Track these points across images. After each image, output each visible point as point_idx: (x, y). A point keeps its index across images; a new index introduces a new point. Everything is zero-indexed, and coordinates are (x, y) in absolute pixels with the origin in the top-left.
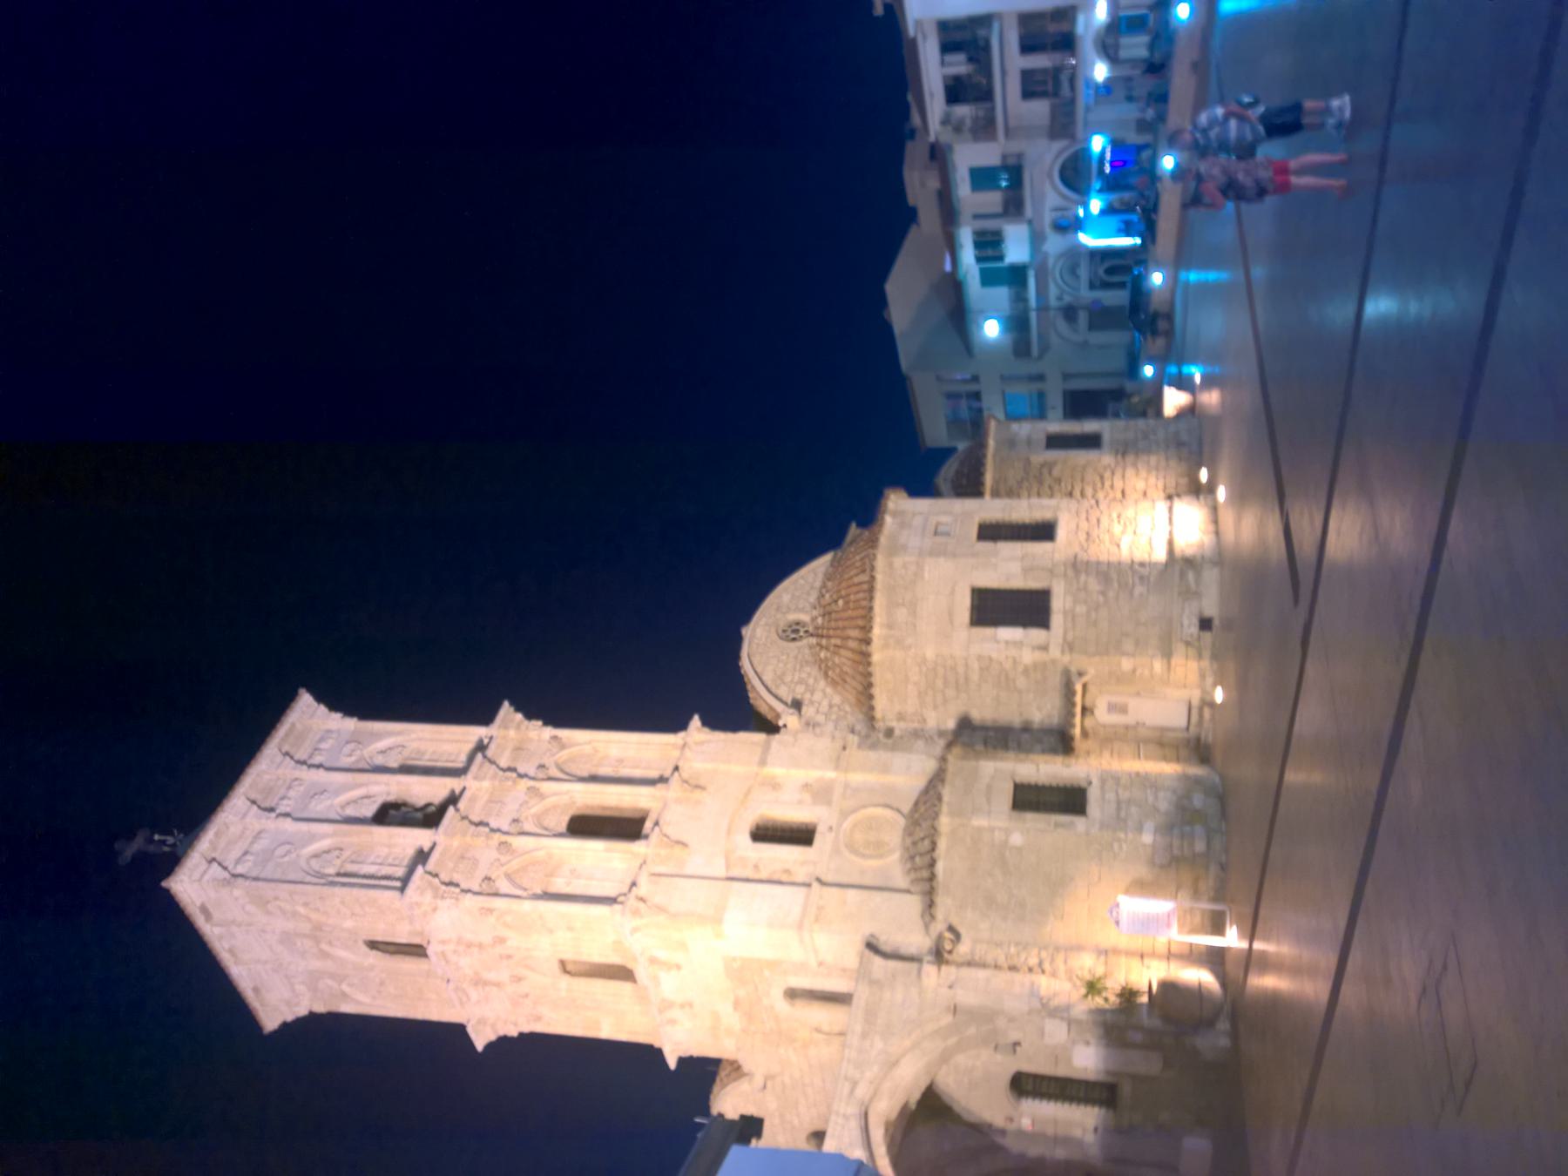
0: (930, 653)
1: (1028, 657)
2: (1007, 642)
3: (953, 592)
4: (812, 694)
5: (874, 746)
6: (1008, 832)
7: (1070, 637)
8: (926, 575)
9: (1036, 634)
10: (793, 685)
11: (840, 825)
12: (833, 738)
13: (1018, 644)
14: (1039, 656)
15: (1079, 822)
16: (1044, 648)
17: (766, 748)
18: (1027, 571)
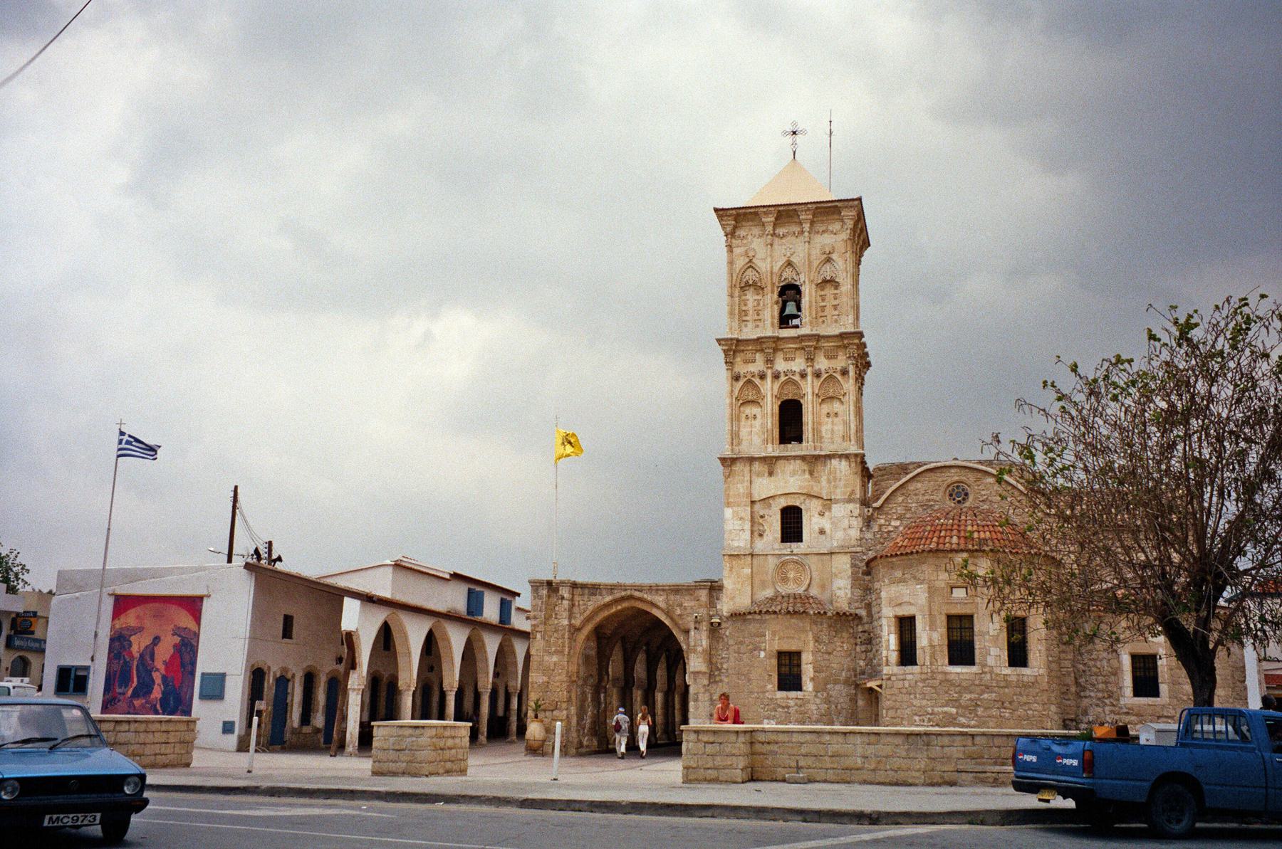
0: (883, 594)
1: (884, 653)
2: (889, 641)
3: (911, 604)
4: (897, 519)
5: (853, 566)
6: (765, 650)
7: (893, 678)
8: (919, 586)
9: (894, 657)
11: (795, 555)
12: (861, 539)
13: (888, 649)
14: (884, 659)
15: (772, 685)
16: (887, 665)
17: (850, 501)
18: (923, 648)
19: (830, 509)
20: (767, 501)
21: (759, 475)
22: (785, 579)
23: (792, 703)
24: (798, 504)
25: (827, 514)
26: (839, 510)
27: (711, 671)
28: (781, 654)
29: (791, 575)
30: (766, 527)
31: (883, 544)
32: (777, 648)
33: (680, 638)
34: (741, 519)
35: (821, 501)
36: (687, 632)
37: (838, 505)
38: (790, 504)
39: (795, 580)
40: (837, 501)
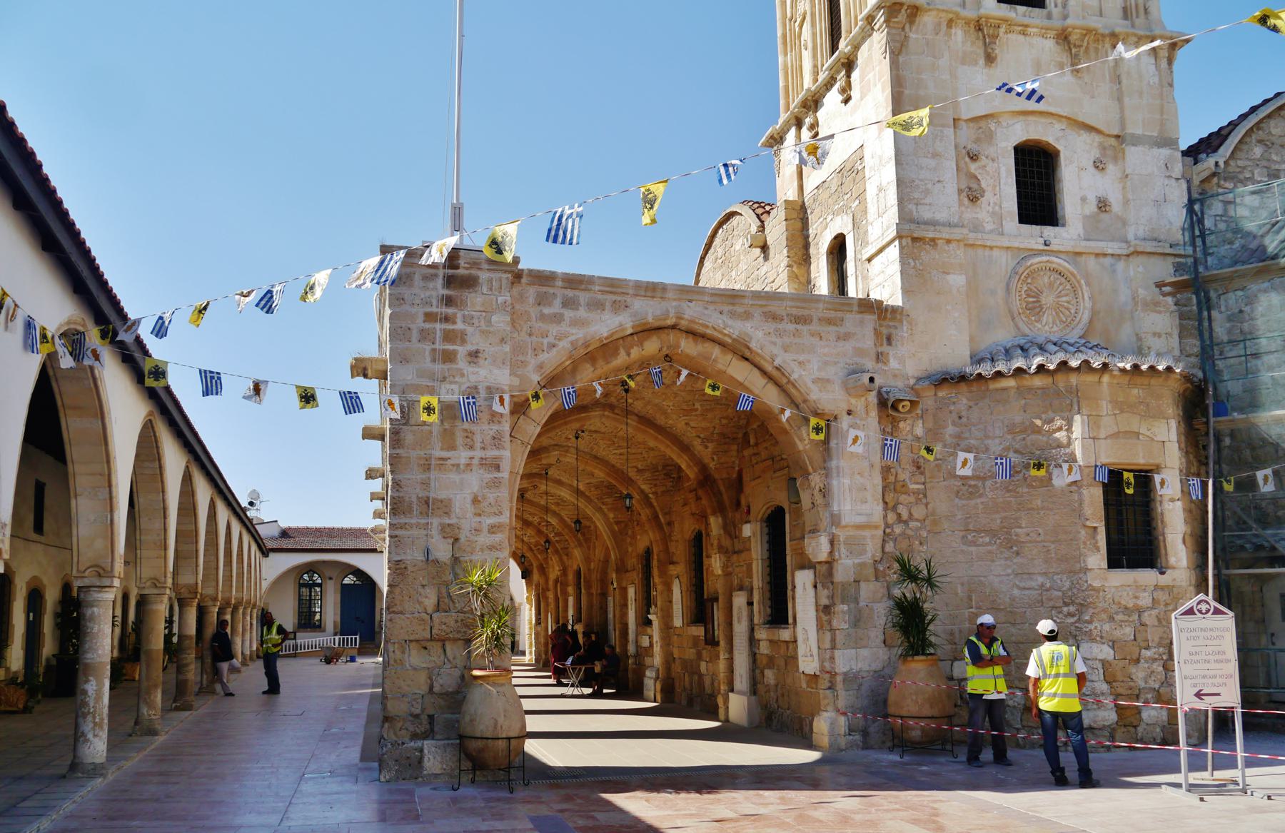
10: (1264, 163)
11: (1056, 253)
19: (1118, 156)
20: (983, 124)
21: (965, 60)
22: (1035, 308)
23: (1145, 600)
24: (1051, 140)
25: (1111, 168)
26: (1141, 160)
27: (887, 525)
28: (1114, 481)
29: (1048, 299)
30: (983, 185)
31: (1231, 243)
32: (1104, 459)
33: (806, 440)
34: (935, 155)
35: (1098, 138)
36: (828, 425)
37: (1140, 148)
38: (1034, 135)
39: (1058, 308)
40: (1136, 141)
